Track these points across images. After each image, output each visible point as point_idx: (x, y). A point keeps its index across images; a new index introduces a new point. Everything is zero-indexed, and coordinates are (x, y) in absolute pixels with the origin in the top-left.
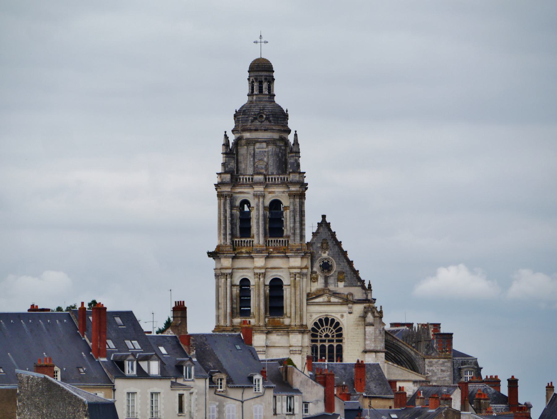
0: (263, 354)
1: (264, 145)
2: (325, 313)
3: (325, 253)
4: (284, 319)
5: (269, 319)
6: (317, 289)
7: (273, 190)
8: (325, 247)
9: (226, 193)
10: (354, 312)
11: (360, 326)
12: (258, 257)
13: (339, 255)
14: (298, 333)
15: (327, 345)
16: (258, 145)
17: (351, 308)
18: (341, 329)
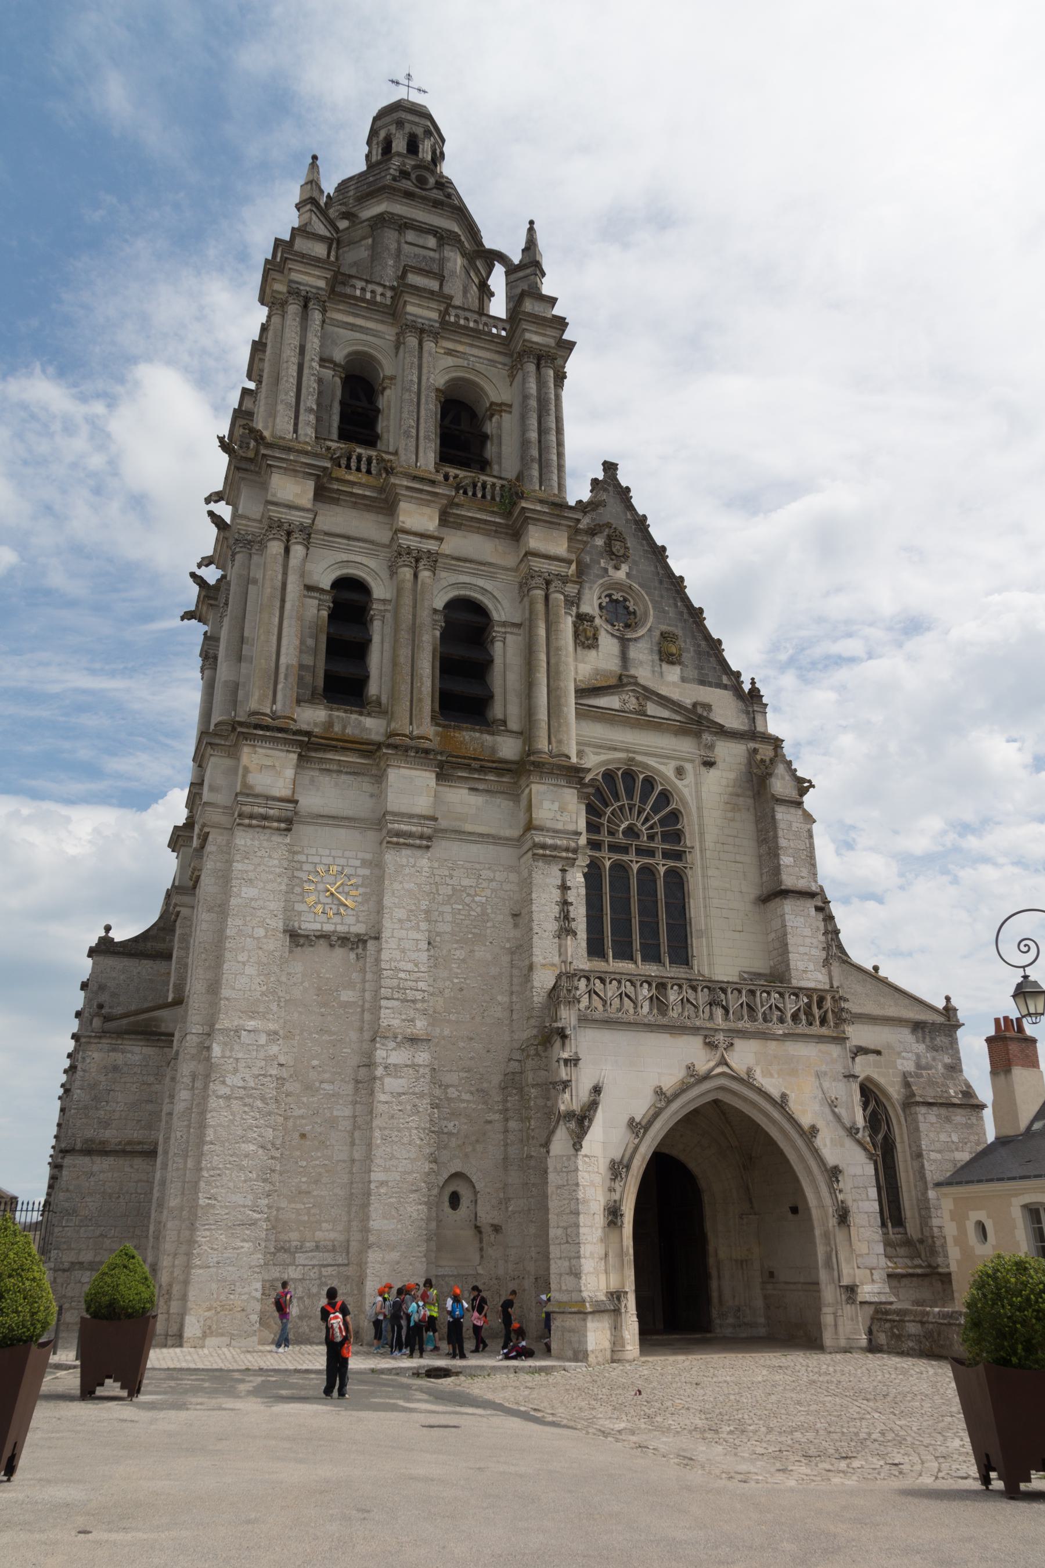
0: (420, 847)
1: (432, 242)
2: (628, 751)
4: (499, 739)
5: (440, 729)
7: (460, 348)
8: (618, 551)
9: (308, 289)
10: (720, 764)
11: (739, 810)
12: (415, 495)
13: (661, 582)
14: (563, 783)
15: (635, 863)
16: (411, 236)
17: (711, 747)
18: (675, 816)
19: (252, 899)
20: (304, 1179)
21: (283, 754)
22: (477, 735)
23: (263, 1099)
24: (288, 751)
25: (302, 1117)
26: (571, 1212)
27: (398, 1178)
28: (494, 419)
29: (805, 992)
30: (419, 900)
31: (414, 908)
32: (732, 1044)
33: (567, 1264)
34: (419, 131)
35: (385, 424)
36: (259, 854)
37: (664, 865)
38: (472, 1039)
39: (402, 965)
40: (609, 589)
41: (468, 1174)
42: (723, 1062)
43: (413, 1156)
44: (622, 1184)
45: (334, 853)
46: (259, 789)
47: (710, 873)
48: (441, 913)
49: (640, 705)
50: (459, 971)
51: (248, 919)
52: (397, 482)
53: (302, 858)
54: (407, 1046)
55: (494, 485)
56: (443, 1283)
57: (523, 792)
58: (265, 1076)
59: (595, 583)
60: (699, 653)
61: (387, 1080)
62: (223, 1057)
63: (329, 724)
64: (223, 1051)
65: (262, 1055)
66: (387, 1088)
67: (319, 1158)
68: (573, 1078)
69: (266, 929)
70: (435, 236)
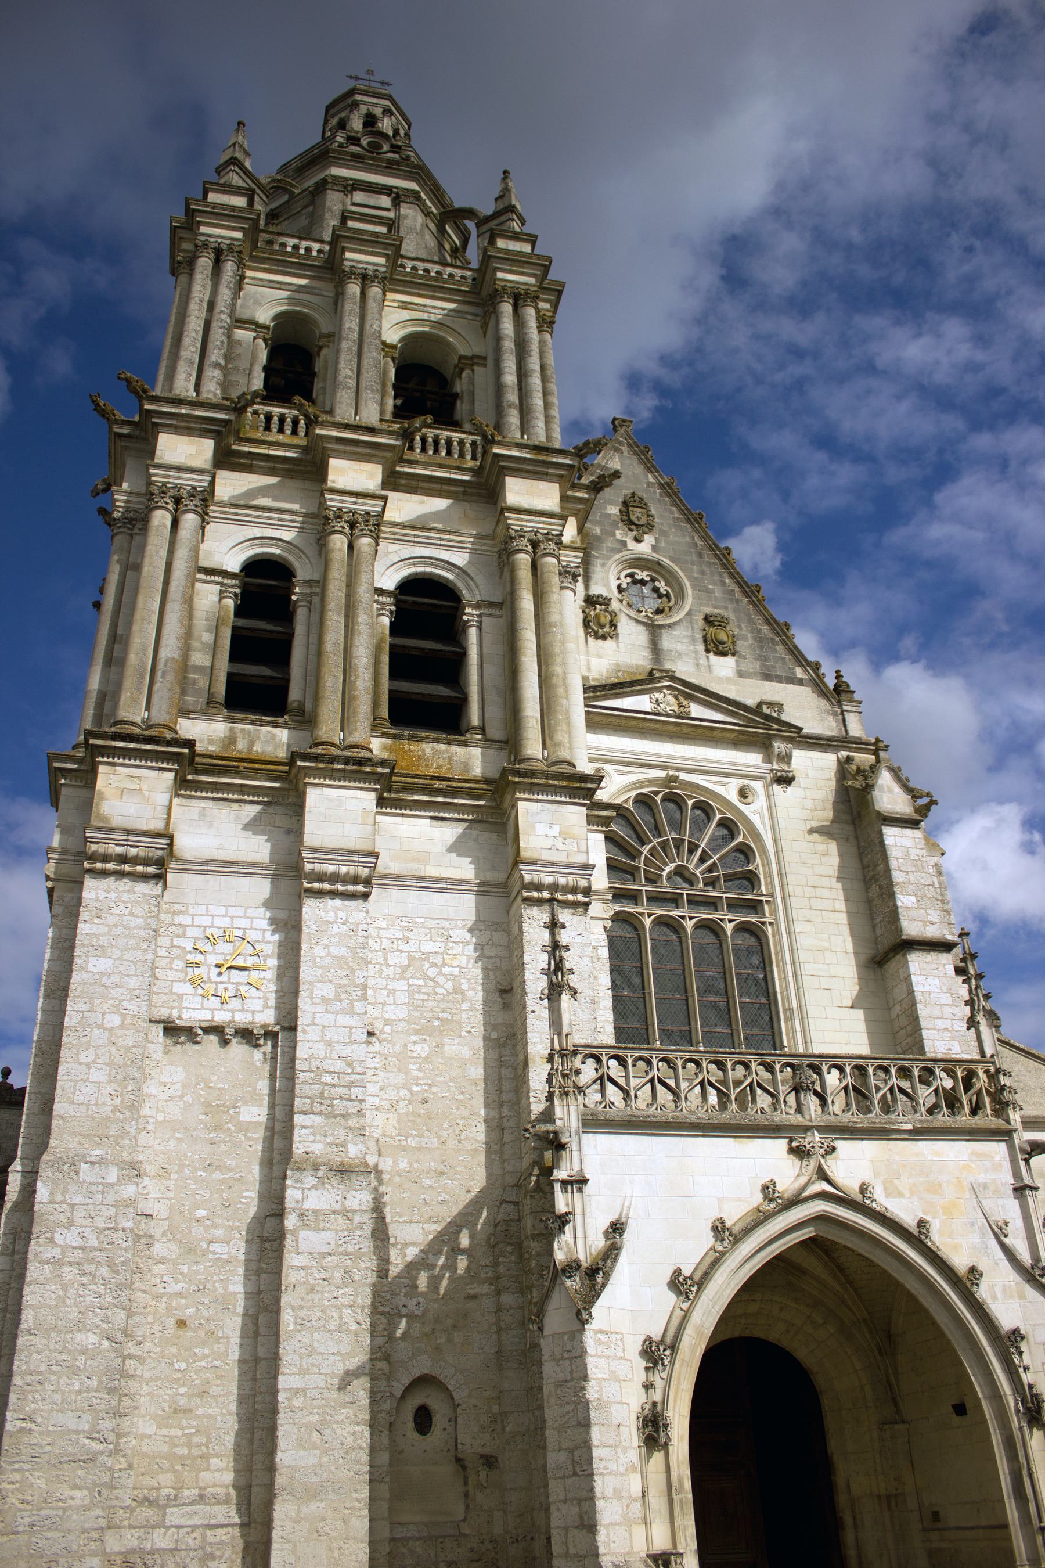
0: (353, 896)
3: (638, 540)
5: (389, 741)
6: (617, 665)
9: (219, 240)
10: (800, 779)
15: (689, 919)
17: (786, 758)
19: (103, 974)
20: (182, 1390)
21: (154, 774)
22: (443, 747)
23: (112, 1265)
24: (161, 769)
25: (180, 1295)
26: (579, 1424)
27: (322, 1384)
28: (464, 375)
29: (942, 1065)
30: (353, 971)
31: (345, 982)
32: (834, 1149)
33: (575, 1510)
34: (378, 111)
35: (320, 385)
36: (116, 911)
37: (730, 921)
38: (442, 1173)
39: (328, 1065)
40: (630, 567)
41: (442, 1378)
42: (822, 1175)
43: (345, 1348)
44: (664, 1375)
45: (232, 911)
46: (116, 822)
47: (798, 927)
48: (392, 992)
49: (680, 705)
50: (421, 1075)
51: (97, 1001)
52: (324, 432)
53: (186, 920)
54: (334, 1182)
55: (461, 442)
56: (404, 1550)
57: (508, 818)
58: (114, 1229)
59: (609, 558)
60: (760, 640)
61: (303, 1234)
62: (51, 1202)
63: (231, 740)
64: (52, 1194)
65: (110, 1198)
66: (303, 1246)
67: (207, 1356)
68: (578, 1210)
69: (122, 1015)
70: (389, 195)
